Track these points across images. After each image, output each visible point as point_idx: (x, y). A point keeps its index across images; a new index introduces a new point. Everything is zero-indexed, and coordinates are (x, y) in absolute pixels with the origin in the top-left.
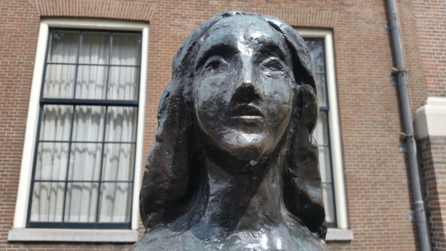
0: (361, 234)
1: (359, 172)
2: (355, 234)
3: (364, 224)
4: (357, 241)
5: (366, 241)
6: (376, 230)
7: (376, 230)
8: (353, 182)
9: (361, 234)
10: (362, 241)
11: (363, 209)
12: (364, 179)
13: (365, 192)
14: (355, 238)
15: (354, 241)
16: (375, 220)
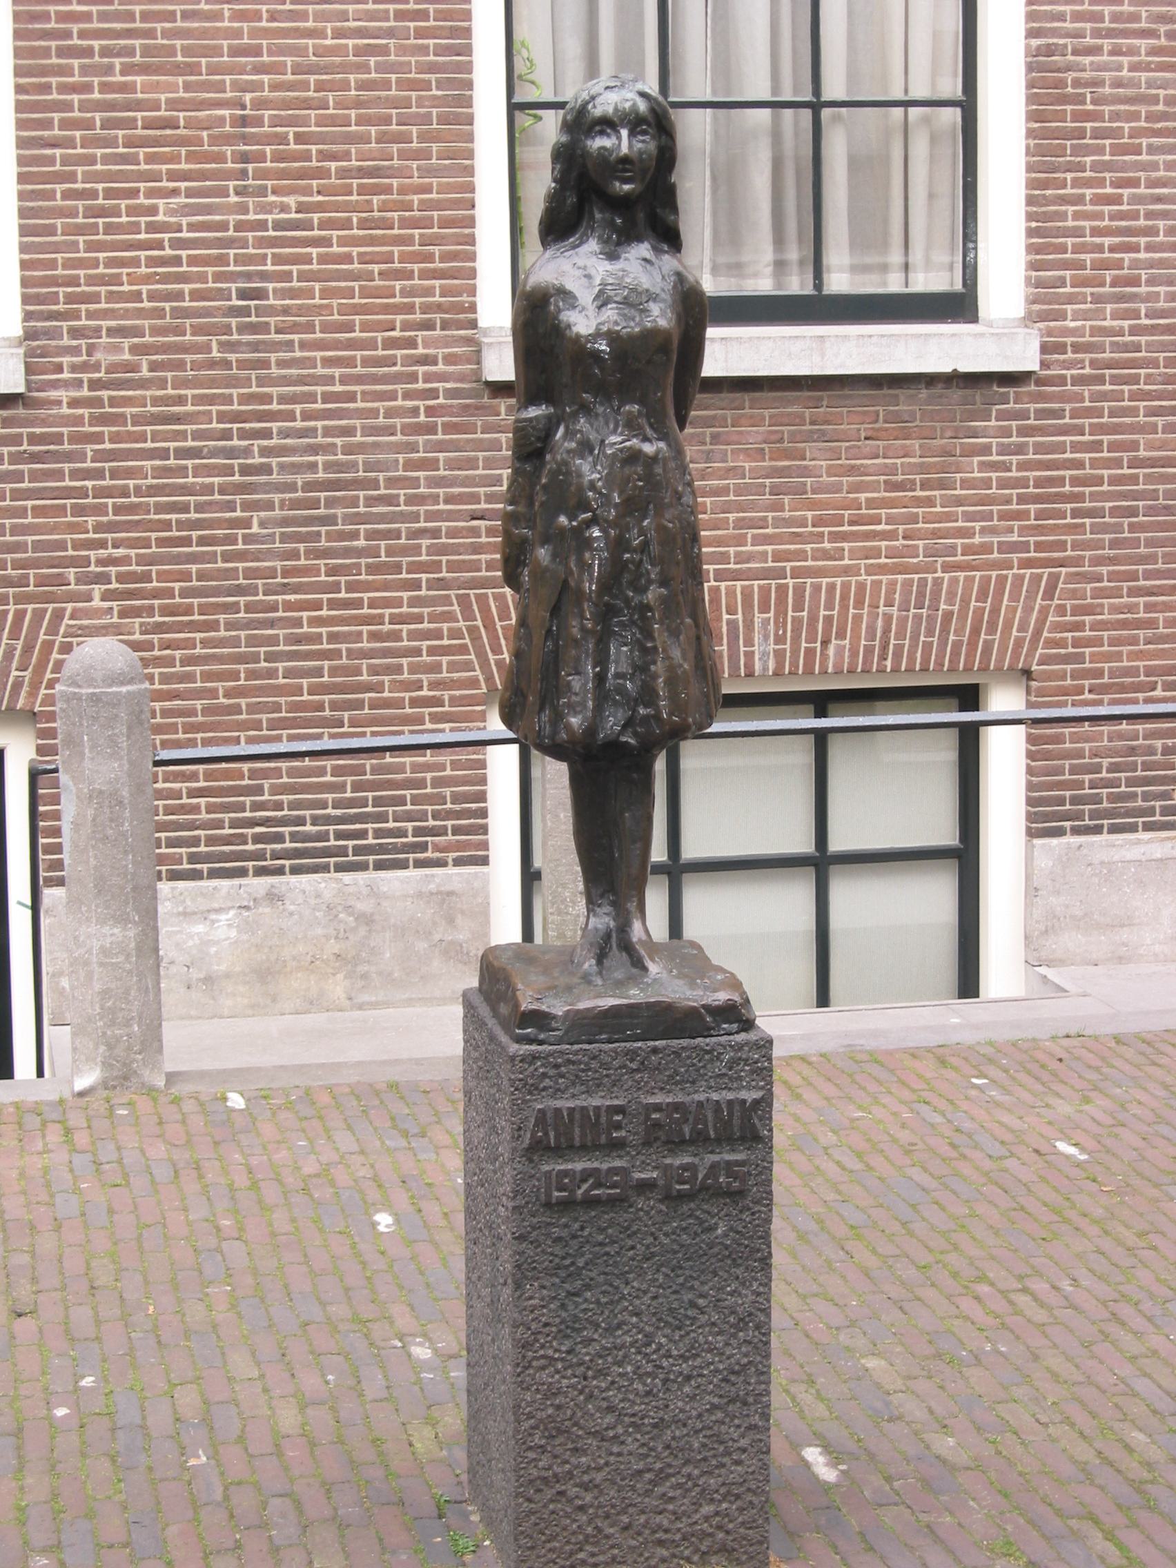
0: (1077, 348)
1: (1096, 50)
2: (1044, 349)
3: (1097, 299)
4: (1062, 381)
5: (1100, 380)
6: (1152, 330)
7: (1152, 330)
8: (1064, 99)
9: (1077, 348)
10: (1078, 381)
11: (1096, 232)
12: (1118, 84)
13: (1119, 150)
14: (1044, 365)
15: (1041, 382)
16: (1151, 281)
